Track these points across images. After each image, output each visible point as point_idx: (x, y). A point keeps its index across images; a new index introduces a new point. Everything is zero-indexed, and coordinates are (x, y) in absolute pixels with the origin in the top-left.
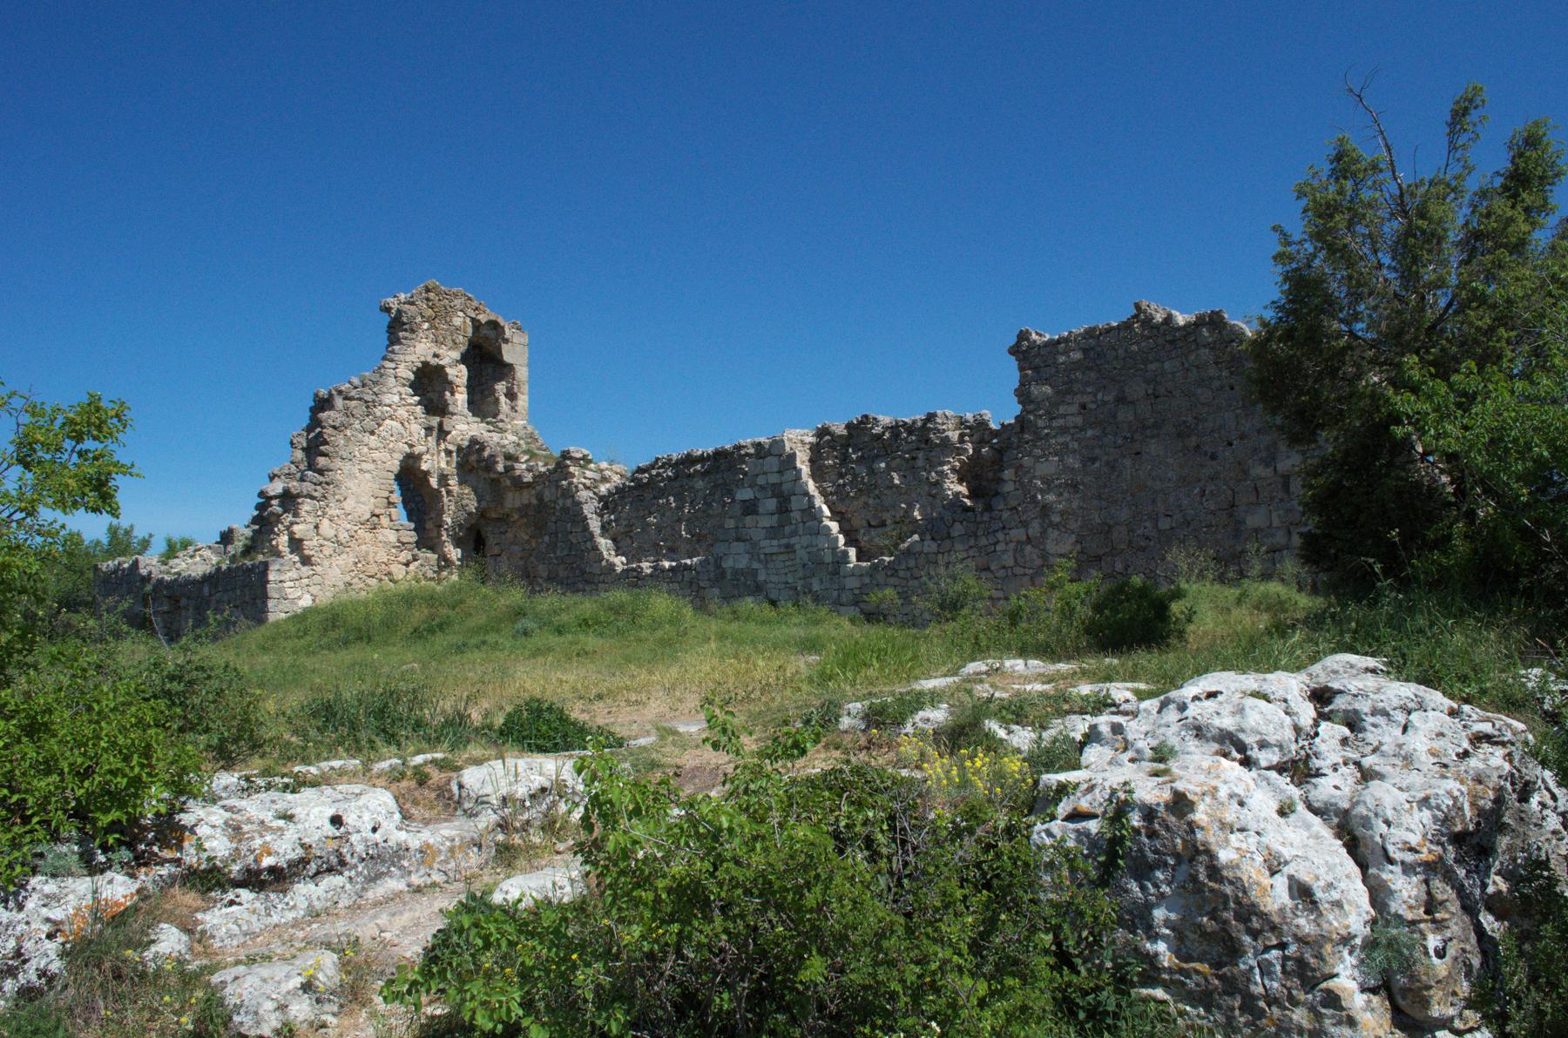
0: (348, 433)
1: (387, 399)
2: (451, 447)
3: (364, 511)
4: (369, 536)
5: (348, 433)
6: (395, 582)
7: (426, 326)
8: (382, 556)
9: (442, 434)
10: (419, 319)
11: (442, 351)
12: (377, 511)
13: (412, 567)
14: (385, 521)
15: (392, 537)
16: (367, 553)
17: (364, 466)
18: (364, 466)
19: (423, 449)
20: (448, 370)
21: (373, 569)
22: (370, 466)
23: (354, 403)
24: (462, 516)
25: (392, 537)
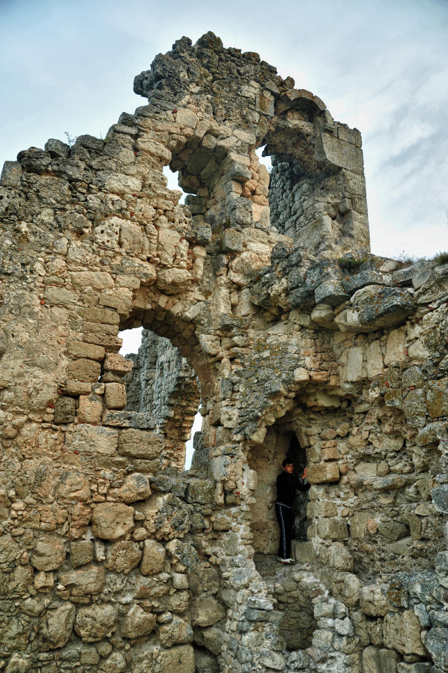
0: (24, 226)
1: (115, 182)
2: (238, 278)
3: (44, 383)
4: (47, 438)
5: (24, 226)
6: (107, 542)
7: (195, 89)
8: (77, 483)
9: (220, 254)
10: (183, 75)
11: (224, 128)
12: (74, 386)
13: (151, 511)
14: (89, 407)
15: (104, 441)
16: (41, 476)
17: (53, 292)
18: (53, 292)
19: (185, 274)
20: (233, 156)
21: (51, 514)
22: (69, 296)
23: (44, 179)
24: (256, 400)
25: (104, 441)
